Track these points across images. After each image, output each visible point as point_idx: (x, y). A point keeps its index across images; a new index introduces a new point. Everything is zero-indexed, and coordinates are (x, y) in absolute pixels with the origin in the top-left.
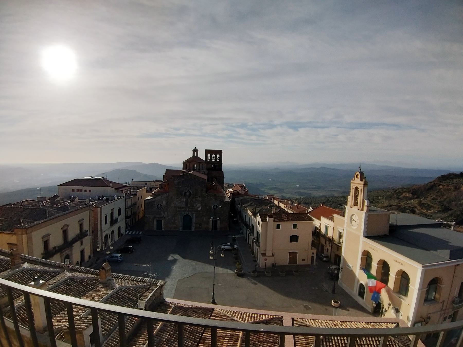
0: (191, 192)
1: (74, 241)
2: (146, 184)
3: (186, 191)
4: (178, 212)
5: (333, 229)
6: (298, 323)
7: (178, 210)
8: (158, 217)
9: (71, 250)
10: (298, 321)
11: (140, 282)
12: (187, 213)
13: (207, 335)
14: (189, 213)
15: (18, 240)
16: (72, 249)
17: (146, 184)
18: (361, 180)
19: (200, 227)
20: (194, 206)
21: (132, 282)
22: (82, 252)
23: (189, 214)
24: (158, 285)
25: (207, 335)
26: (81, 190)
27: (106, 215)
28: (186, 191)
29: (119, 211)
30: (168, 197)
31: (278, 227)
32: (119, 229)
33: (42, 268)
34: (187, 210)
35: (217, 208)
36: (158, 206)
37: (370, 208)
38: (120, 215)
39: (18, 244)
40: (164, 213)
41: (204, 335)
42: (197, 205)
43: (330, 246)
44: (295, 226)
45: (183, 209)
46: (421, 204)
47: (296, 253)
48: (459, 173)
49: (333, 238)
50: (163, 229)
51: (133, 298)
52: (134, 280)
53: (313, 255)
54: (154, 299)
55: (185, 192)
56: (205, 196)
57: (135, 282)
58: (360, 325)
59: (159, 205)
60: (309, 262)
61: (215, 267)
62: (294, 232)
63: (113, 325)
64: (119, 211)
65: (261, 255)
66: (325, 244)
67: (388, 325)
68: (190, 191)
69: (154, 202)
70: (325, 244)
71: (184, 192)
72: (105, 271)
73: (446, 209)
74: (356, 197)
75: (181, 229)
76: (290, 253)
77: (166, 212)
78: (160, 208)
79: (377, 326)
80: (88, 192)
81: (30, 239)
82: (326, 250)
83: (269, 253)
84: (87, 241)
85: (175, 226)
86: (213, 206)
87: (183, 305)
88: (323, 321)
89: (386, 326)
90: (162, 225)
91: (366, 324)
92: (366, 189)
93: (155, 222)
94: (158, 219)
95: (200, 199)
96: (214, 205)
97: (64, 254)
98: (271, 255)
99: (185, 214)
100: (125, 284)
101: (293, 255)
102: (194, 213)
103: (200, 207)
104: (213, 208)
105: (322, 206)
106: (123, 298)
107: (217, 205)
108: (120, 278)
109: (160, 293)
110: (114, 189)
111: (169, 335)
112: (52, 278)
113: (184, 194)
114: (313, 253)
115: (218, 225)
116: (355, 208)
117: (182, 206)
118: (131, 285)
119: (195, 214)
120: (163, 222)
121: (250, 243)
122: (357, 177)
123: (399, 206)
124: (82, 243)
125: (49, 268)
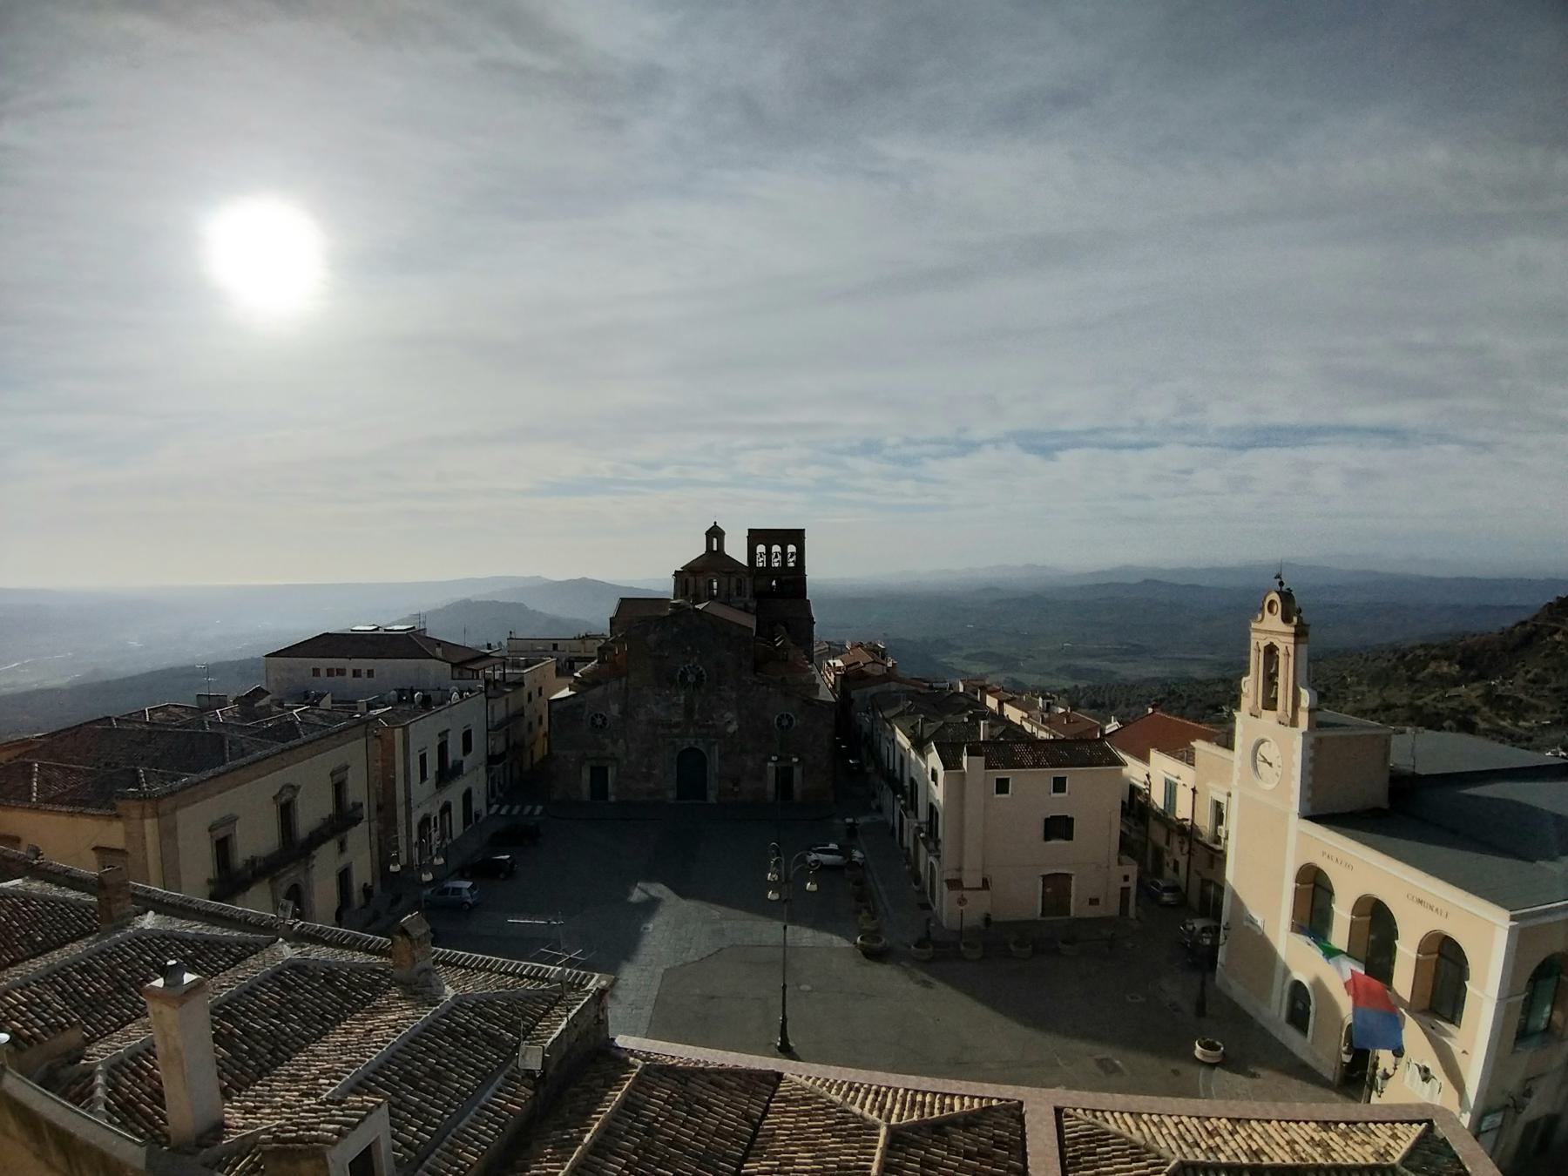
0: (701, 672)
1: (318, 838)
2: (555, 646)
3: (685, 668)
5: (1192, 792)
6: (1077, 1126)
9: (307, 871)
10: (1077, 1119)
11: (528, 977)
12: (692, 743)
13: (756, 1167)
14: (696, 742)
15: (128, 835)
16: (310, 866)
17: (555, 646)
18: (1286, 619)
19: (736, 789)
20: (712, 719)
21: (502, 978)
22: (344, 877)
23: (696, 747)
24: (590, 991)
25: (756, 1167)
26: (341, 672)
27: (422, 753)
28: (685, 668)
29: (467, 737)
30: (627, 688)
31: (1002, 786)
32: (467, 797)
33: (201, 932)
36: (593, 719)
37: (1320, 716)
38: (470, 750)
39: (129, 850)
40: (615, 742)
41: (745, 1165)
42: (722, 716)
43: (1186, 848)
44: (1059, 785)
45: (676, 731)
47: (1068, 877)
49: (1193, 822)
50: (612, 798)
51: (501, 1034)
52: (506, 973)
53: (1126, 884)
54: (577, 1040)
55: (682, 672)
57: (510, 980)
58: (1302, 1132)
60: (1113, 909)
61: (785, 928)
62: (1058, 805)
63: (434, 1129)
64: (467, 737)
65: (945, 884)
66: (1168, 843)
67: (1396, 1131)
68: (701, 669)
69: (580, 706)
70: (1168, 843)
71: (679, 673)
72: (411, 941)
74: (1270, 679)
76: (1045, 878)
77: (621, 741)
78: (601, 727)
79: (1359, 1133)
81: (168, 834)
82: (1172, 865)
83: (971, 879)
84: (359, 838)
85: (652, 785)
86: (777, 717)
87: (675, 1061)
88: (1166, 1120)
89: (1390, 1133)
91: (1320, 1129)
92: (1303, 648)
93: (586, 775)
94: (594, 763)
96: (782, 716)
97: (284, 885)
98: (980, 886)
99: (683, 746)
100: (478, 985)
101: (1057, 886)
102: (714, 743)
103: (735, 723)
104: (779, 724)
105: (1154, 712)
106: (468, 1033)
107: (790, 714)
108: (462, 966)
109: (597, 1016)
110: (450, 665)
111: (625, 1167)
112: (233, 966)
113: (678, 678)
114: (1126, 878)
115: (795, 785)
116: (1269, 717)
117: (676, 719)
118: (498, 988)
119: (717, 747)
120: (611, 772)
121: (905, 844)
122: (1270, 611)
124: (342, 847)
125: (225, 930)
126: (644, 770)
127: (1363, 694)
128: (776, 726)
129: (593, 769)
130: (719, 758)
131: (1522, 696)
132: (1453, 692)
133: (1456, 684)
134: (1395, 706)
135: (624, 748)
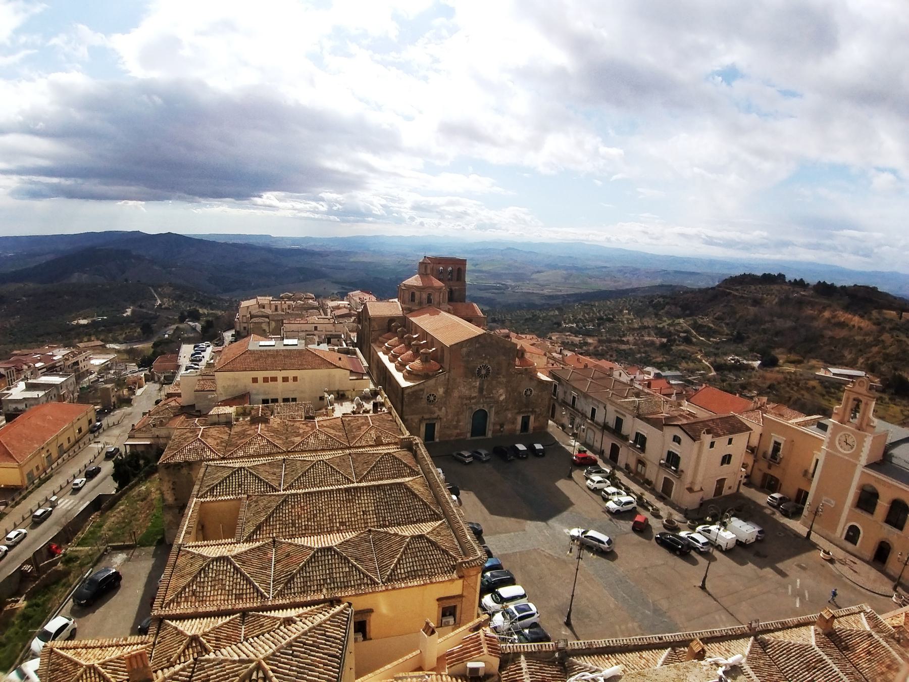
2: (316, 328)
4: (465, 407)
5: (759, 436)
7: (465, 402)
8: (429, 419)
17: (316, 328)
20: (493, 394)
26: (274, 379)
34: (481, 400)
36: (428, 397)
40: (440, 409)
44: (730, 442)
45: (473, 401)
46: (698, 328)
50: (437, 440)
56: (513, 373)
59: (430, 395)
62: (729, 449)
69: (422, 390)
73: (739, 339)
75: (469, 435)
77: (443, 408)
80: (291, 381)
83: (696, 488)
85: (458, 431)
90: (436, 433)
94: (428, 422)
95: (504, 380)
101: (721, 482)
119: (493, 409)
120: (437, 427)
123: (660, 329)
126: (455, 423)
128: (525, 396)
131: (711, 325)
132: (677, 321)
133: (679, 317)
134: (648, 327)
135: (445, 412)
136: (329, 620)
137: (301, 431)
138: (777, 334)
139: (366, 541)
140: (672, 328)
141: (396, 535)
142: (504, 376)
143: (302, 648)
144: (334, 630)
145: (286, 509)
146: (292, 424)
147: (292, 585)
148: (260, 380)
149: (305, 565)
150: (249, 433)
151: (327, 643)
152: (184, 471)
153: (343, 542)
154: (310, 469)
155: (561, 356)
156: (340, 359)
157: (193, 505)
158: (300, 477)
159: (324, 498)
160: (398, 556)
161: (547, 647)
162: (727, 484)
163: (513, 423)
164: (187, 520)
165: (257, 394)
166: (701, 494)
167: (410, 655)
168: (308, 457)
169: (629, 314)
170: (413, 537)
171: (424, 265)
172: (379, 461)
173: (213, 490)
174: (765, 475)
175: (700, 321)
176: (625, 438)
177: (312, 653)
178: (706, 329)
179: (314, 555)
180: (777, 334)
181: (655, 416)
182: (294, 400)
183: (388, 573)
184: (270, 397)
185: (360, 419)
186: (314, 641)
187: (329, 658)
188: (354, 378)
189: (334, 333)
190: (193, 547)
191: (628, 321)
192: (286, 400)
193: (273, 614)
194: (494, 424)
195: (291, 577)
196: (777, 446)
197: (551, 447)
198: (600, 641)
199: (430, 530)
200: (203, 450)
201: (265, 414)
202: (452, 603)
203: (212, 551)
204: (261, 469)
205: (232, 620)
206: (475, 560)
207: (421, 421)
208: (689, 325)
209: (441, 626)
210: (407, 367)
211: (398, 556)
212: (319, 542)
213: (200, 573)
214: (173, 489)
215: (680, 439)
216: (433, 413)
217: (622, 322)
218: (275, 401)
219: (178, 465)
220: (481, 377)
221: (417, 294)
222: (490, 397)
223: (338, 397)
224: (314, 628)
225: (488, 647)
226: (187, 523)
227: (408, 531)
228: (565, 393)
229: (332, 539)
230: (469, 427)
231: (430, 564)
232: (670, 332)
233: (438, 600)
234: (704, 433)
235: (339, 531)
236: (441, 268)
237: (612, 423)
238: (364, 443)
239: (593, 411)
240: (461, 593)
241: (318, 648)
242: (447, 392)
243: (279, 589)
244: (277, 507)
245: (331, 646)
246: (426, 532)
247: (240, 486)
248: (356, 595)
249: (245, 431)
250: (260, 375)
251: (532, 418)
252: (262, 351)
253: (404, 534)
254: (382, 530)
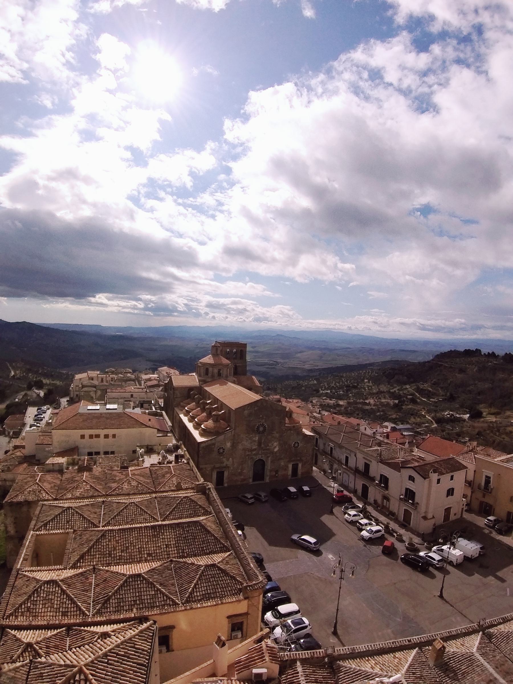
2: (132, 396)
5: (473, 472)
7: (247, 453)
14: (262, 457)
17: (132, 396)
26: (98, 436)
30: (234, 435)
31: (439, 481)
34: (260, 452)
35: (298, 446)
40: (228, 460)
42: (273, 445)
44: (452, 478)
45: (254, 452)
46: (421, 391)
48: (462, 349)
50: (226, 485)
56: (284, 430)
62: (450, 484)
69: (214, 444)
73: (452, 398)
75: (251, 480)
83: (430, 516)
85: (242, 477)
90: (225, 479)
94: (218, 470)
95: (278, 435)
115: (299, 471)
117: (254, 447)
120: (226, 474)
123: (393, 393)
127: (371, 386)
129: (217, 472)
130: (271, 462)
132: (404, 387)
133: (406, 384)
134: (384, 392)
136: (137, 635)
137: (117, 478)
138: (479, 394)
139: (168, 570)
140: (401, 392)
141: (193, 564)
142: (277, 433)
143: (116, 657)
144: (142, 643)
145: (104, 542)
146: (110, 472)
147: (108, 605)
148: (87, 437)
149: (118, 589)
150: (76, 479)
151: (136, 654)
152: (25, 509)
153: (149, 570)
154: (123, 509)
155: (320, 415)
156: (150, 420)
157: (30, 537)
158: (115, 516)
159: (135, 534)
160: (195, 582)
161: (318, 653)
162: (452, 512)
163: (286, 470)
164: (25, 549)
165: (84, 448)
166: (433, 521)
167: (206, 664)
168: (123, 500)
169: (369, 382)
170: (207, 566)
171: (215, 348)
172: (179, 503)
173: (47, 525)
174: (481, 503)
175: (421, 387)
176: (373, 479)
177: (124, 662)
178: (426, 392)
179: (126, 581)
180: (479, 394)
181: (393, 461)
182: (113, 453)
183: (187, 596)
184: (94, 450)
185: (164, 468)
186: (125, 652)
187: (138, 666)
188: (161, 435)
189: (146, 400)
190: (28, 571)
191: (368, 388)
192: (106, 453)
193: (93, 629)
194: (271, 471)
195: (107, 599)
196: (488, 479)
197: (317, 488)
198: (361, 646)
199: (220, 560)
200: (40, 492)
201: (89, 464)
202: (239, 620)
203: (44, 575)
204: (85, 509)
205: (59, 633)
206: (257, 584)
207: (214, 468)
208: (413, 390)
209: (231, 639)
210: (202, 426)
211: (195, 582)
212: (131, 569)
213: (33, 593)
214: (15, 523)
215: (414, 478)
216: (222, 462)
217: (364, 388)
218: (98, 453)
219: (19, 504)
220: (259, 433)
221: (210, 369)
222: (267, 449)
223: (148, 450)
224: (125, 641)
225: (270, 656)
226: (25, 551)
227: (203, 561)
228: (324, 444)
229: (141, 567)
230: (251, 474)
231: (220, 588)
232: (400, 395)
233: (228, 617)
234: (431, 472)
235: (146, 561)
236: (228, 350)
237: (361, 467)
238: (167, 488)
239: (347, 458)
240: (246, 611)
241: (129, 657)
242: (234, 446)
243: (97, 608)
244: (97, 540)
245: (139, 657)
246: (217, 562)
247: (68, 522)
248: (161, 614)
249: (73, 477)
250: (87, 432)
251: (300, 465)
252: (89, 414)
253: (199, 563)
254: (181, 560)
